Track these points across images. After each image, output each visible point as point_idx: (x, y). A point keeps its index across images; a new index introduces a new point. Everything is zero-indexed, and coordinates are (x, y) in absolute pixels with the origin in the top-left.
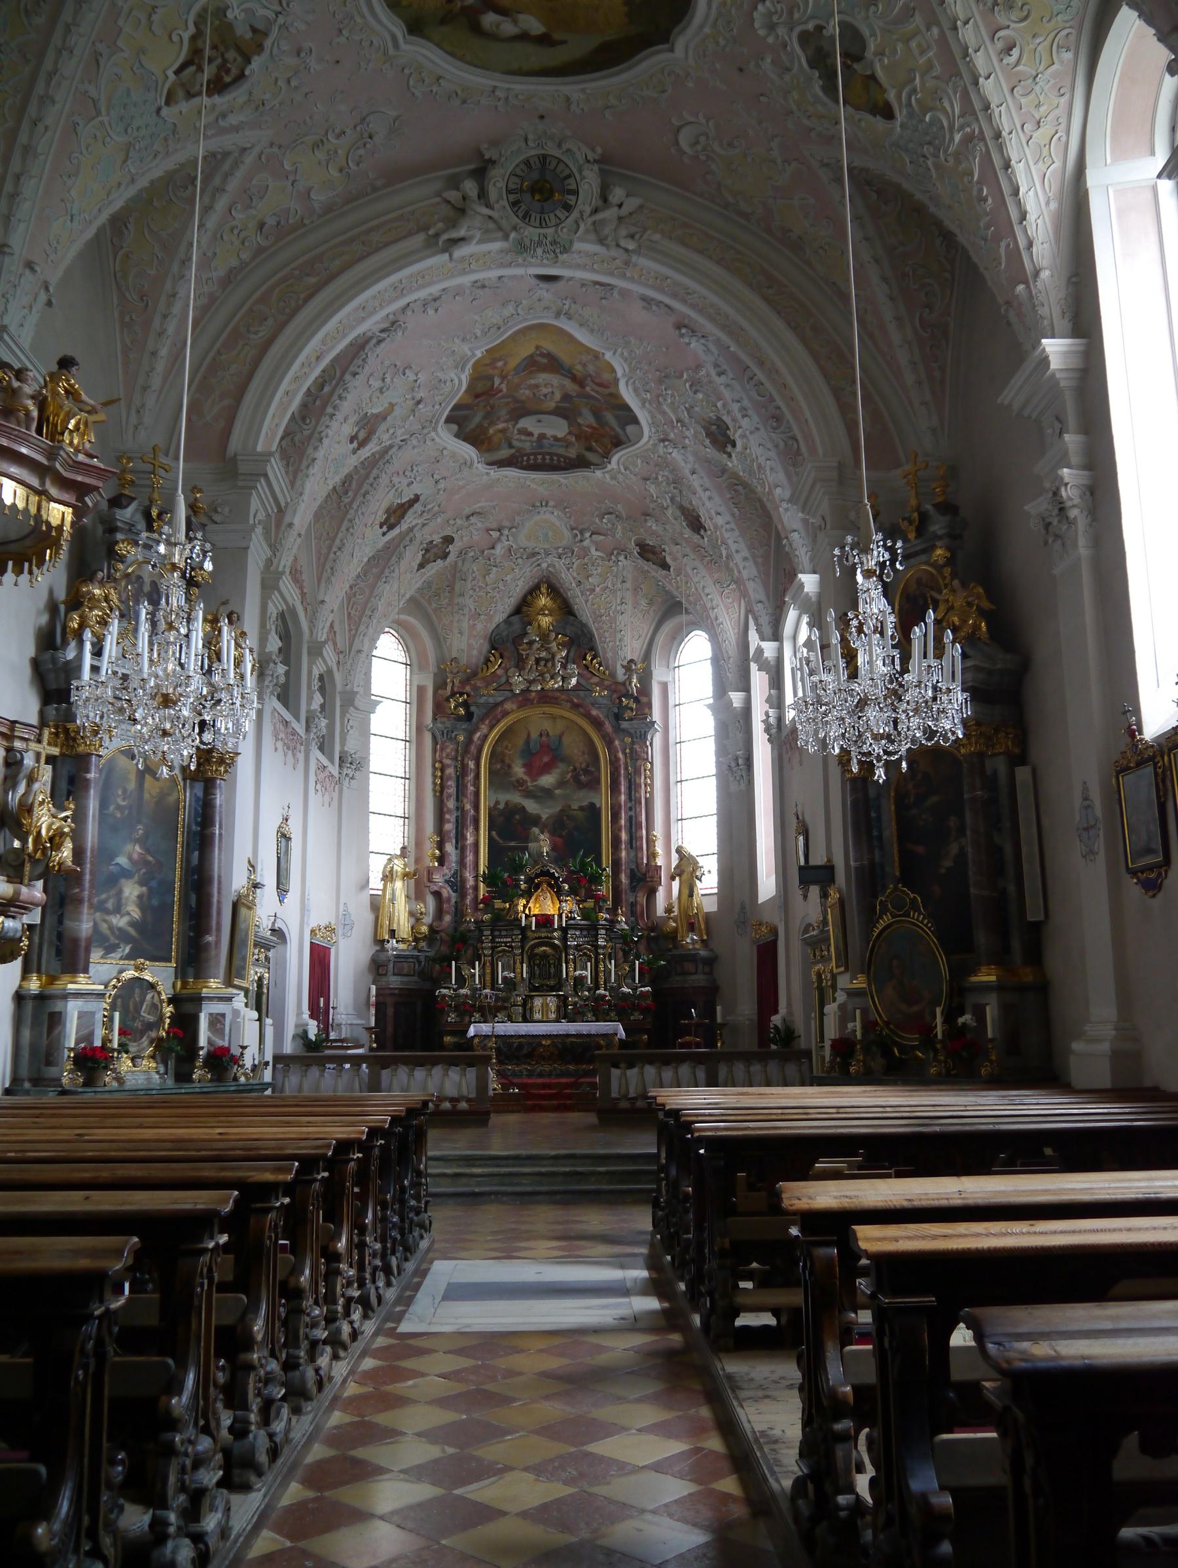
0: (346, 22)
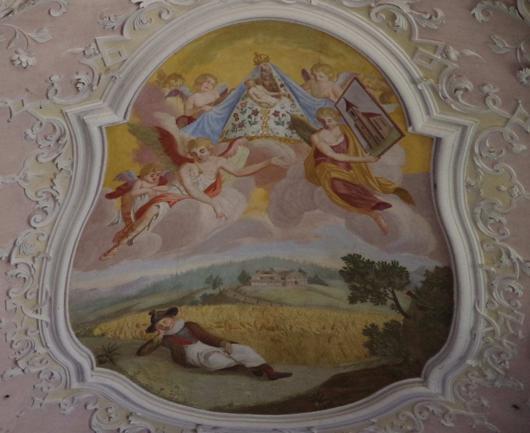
0: (23, 353)
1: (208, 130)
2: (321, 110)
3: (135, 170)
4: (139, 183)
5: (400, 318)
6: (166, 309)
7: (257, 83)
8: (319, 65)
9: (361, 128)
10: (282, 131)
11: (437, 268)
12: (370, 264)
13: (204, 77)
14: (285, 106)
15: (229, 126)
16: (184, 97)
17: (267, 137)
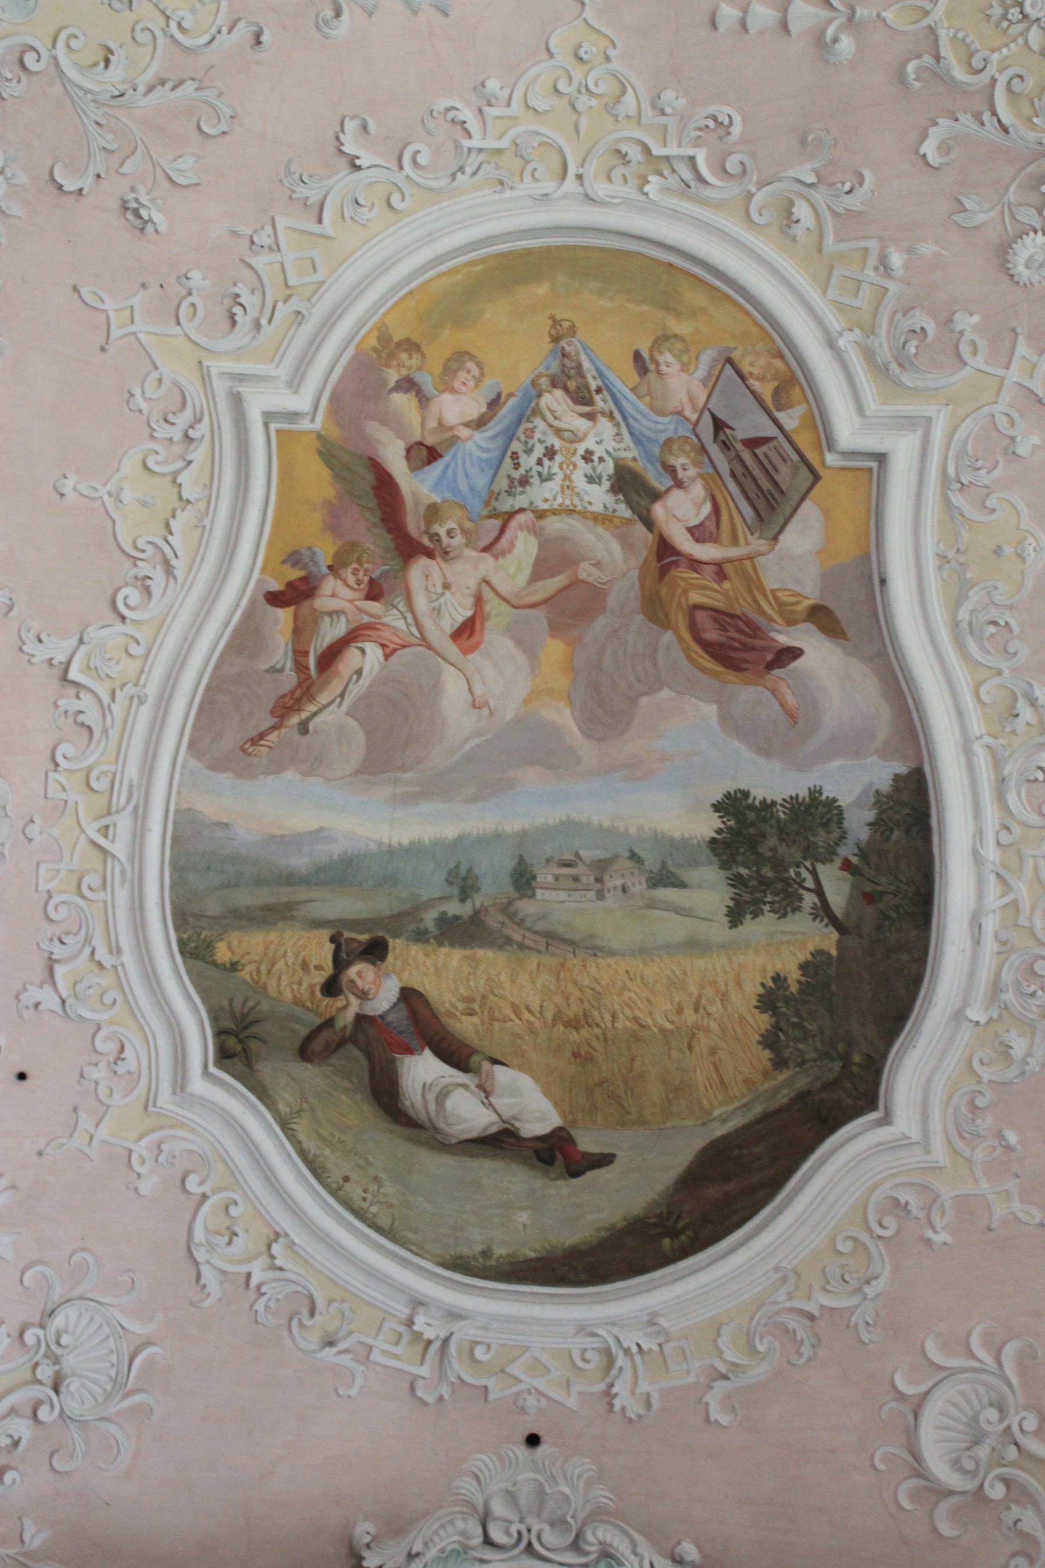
1: (463, 487)
2: (668, 442)
3: (325, 552)
4: (330, 584)
5: (828, 939)
6: (364, 937)
7: (554, 384)
8: (663, 339)
9: (741, 476)
10: (599, 497)
11: (897, 778)
12: (767, 806)
13: (461, 356)
14: (603, 439)
15: (502, 483)
16: (423, 400)
17: (571, 512)
